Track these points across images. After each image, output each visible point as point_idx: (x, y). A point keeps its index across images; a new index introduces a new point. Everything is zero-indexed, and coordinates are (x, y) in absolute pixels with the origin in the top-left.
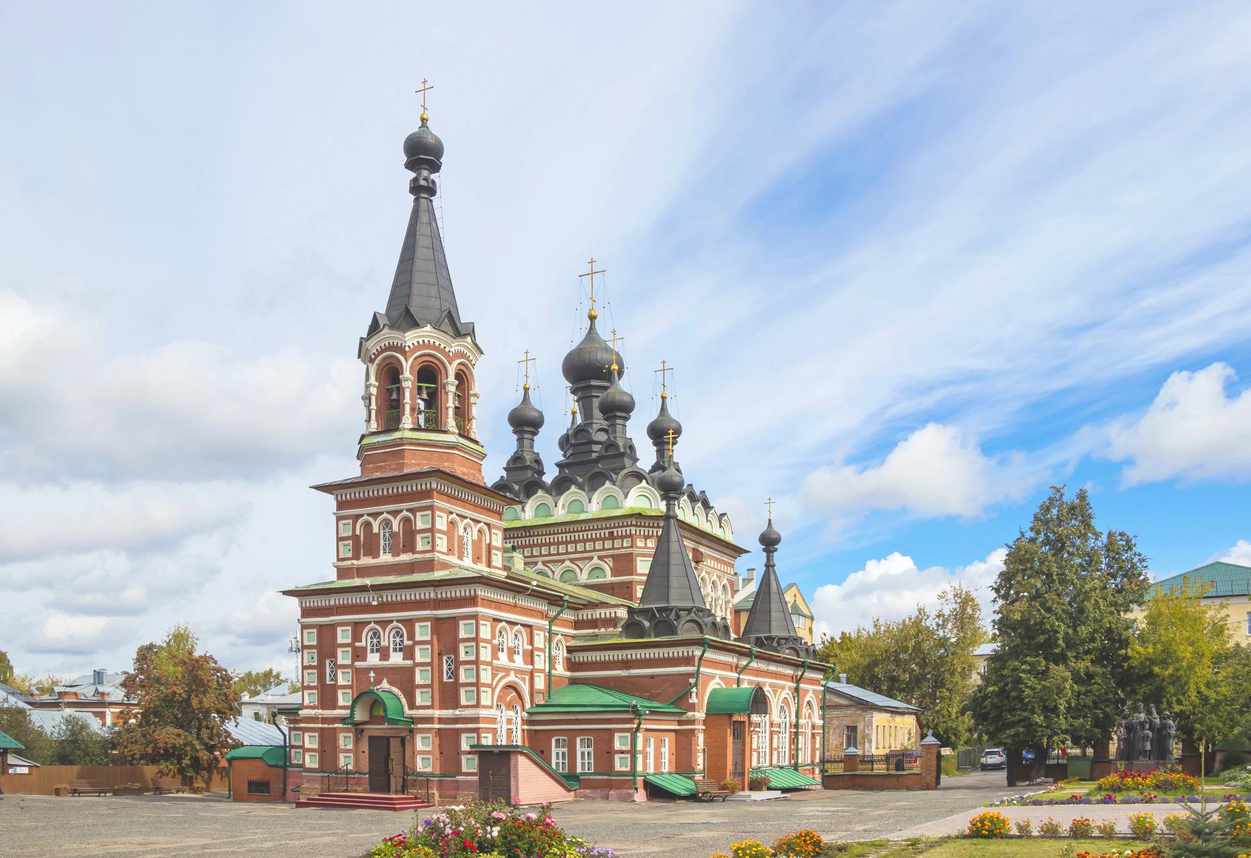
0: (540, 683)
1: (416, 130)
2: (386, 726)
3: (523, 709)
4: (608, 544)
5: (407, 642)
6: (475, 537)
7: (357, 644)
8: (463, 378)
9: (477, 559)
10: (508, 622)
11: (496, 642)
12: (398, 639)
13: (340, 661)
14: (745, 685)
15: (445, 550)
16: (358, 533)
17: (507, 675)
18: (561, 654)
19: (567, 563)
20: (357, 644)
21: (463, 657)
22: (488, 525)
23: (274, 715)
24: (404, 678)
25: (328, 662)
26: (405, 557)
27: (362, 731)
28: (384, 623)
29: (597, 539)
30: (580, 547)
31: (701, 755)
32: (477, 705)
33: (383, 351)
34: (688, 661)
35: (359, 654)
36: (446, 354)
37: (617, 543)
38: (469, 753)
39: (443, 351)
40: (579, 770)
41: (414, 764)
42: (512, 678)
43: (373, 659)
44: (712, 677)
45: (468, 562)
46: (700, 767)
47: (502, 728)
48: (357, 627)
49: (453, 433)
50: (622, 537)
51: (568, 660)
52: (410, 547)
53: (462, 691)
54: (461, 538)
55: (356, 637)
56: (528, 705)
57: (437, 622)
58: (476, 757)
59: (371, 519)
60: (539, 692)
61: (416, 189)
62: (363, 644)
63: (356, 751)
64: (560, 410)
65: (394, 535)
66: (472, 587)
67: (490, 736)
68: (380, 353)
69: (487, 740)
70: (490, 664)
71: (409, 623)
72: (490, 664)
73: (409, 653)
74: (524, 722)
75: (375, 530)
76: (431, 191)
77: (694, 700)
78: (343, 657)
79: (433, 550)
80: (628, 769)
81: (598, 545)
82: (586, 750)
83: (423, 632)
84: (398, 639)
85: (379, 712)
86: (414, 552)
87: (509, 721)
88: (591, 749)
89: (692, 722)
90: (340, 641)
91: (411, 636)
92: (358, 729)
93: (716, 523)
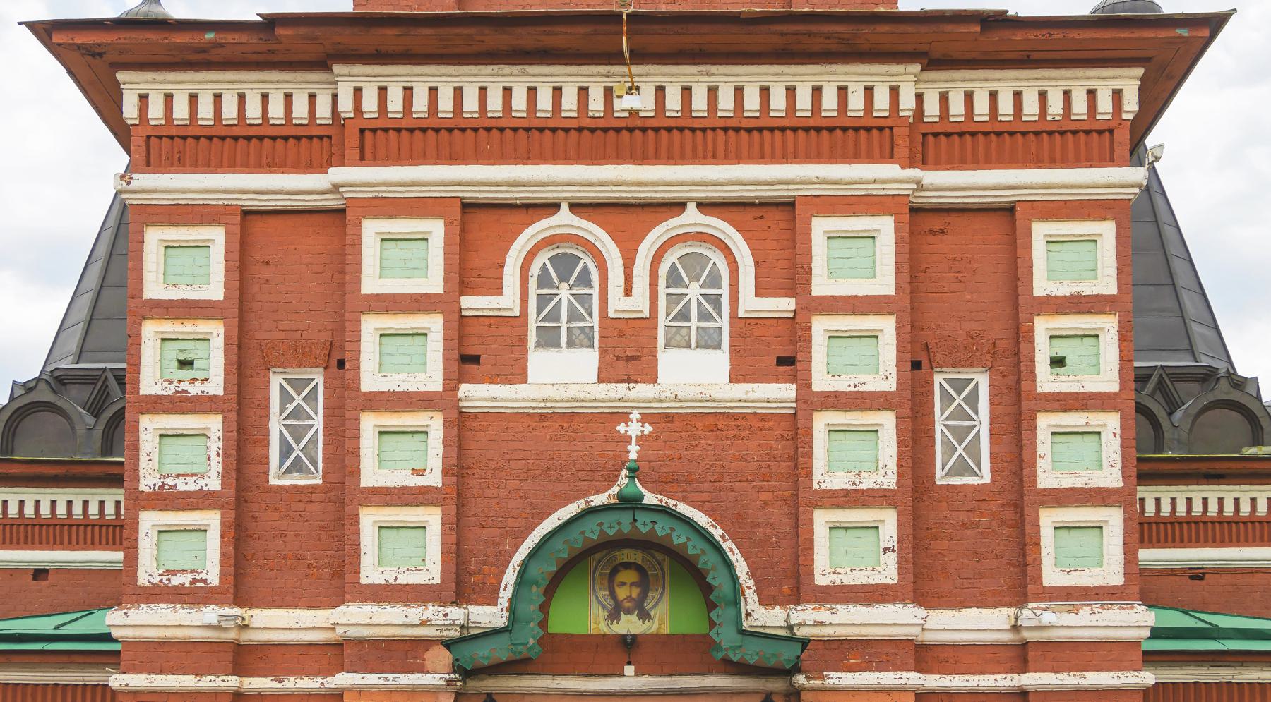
5: (752, 304)
7: (473, 303)
12: (694, 291)
20: (473, 303)
24: (765, 467)
43: (562, 375)
62: (506, 302)
73: (776, 350)
78: (405, 357)
91: (787, 269)
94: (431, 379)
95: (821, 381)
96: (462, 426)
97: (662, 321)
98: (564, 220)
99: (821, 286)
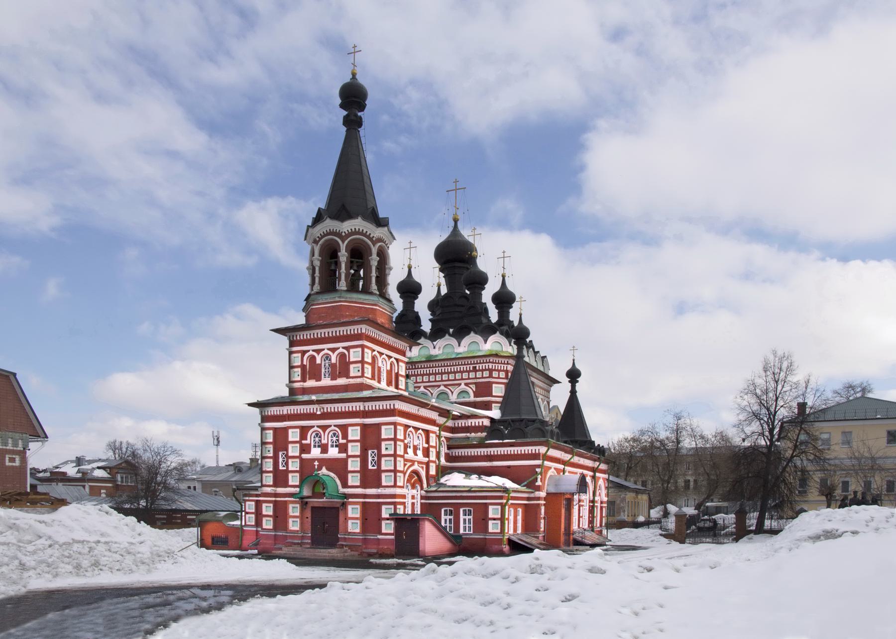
0: (433, 472)
1: (348, 80)
2: (325, 499)
3: (422, 488)
4: (472, 375)
5: (342, 441)
6: (389, 368)
7: (304, 442)
8: (383, 256)
9: (389, 383)
10: (414, 428)
11: (406, 441)
12: (334, 439)
13: (290, 454)
14: (567, 474)
15: (370, 376)
16: (305, 363)
17: (413, 465)
18: (444, 450)
19: (442, 388)
20: (304, 442)
21: (384, 452)
22: (397, 360)
23: (234, 490)
24: (339, 467)
25: (281, 453)
26: (342, 381)
27: (307, 503)
28: (324, 428)
29: (464, 372)
30: (451, 377)
31: (542, 521)
32: (395, 486)
33: (325, 235)
34: (535, 456)
36: (371, 239)
37: (479, 374)
38: (388, 519)
39: (368, 237)
40: (462, 531)
41: (346, 528)
42: (416, 467)
43: (316, 452)
44: (550, 468)
45: (383, 385)
46: (542, 529)
47: (409, 501)
48: (304, 431)
49: (375, 294)
50: (482, 371)
51: (447, 455)
53: (383, 475)
54: (379, 368)
55: (303, 436)
56: (425, 485)
57: (364, 427)
58: (392, 523)
59: (315, 354)
60: (432, 476)
61: (347, 121)
62: (308, 442)
63: (302, 517)
64: (432, 282)
65: (333, 366)
66: (392, 402)
67: (401, 507)
68: (323, 237)
69: (400, 510)
70: (402, 456)
71: (344, 428)
72: (402, 456)
73: (343, 448)
74: (422, 498)
75: (318, 361)
76: (359, 123)
77: (539, 483)
78: (294, 450)
79: (363, 376)
80: (499, 531)
81: (465, 375)
82: (467, 517)
83: (354, 433)
84: (334, 439)
85: (319, 489)
86: (348, 377)
87: (413, 497)
88: (471, 517)
89: (539, 499)
90: (290, 439)
91: (345, 436)
92: (304, 503)
93: (540, 363)
94: (297, 454)
95: (350, 453)
96: (302, 461)
97: (330, 443)
98: (316, 428)
99: (350, 438)
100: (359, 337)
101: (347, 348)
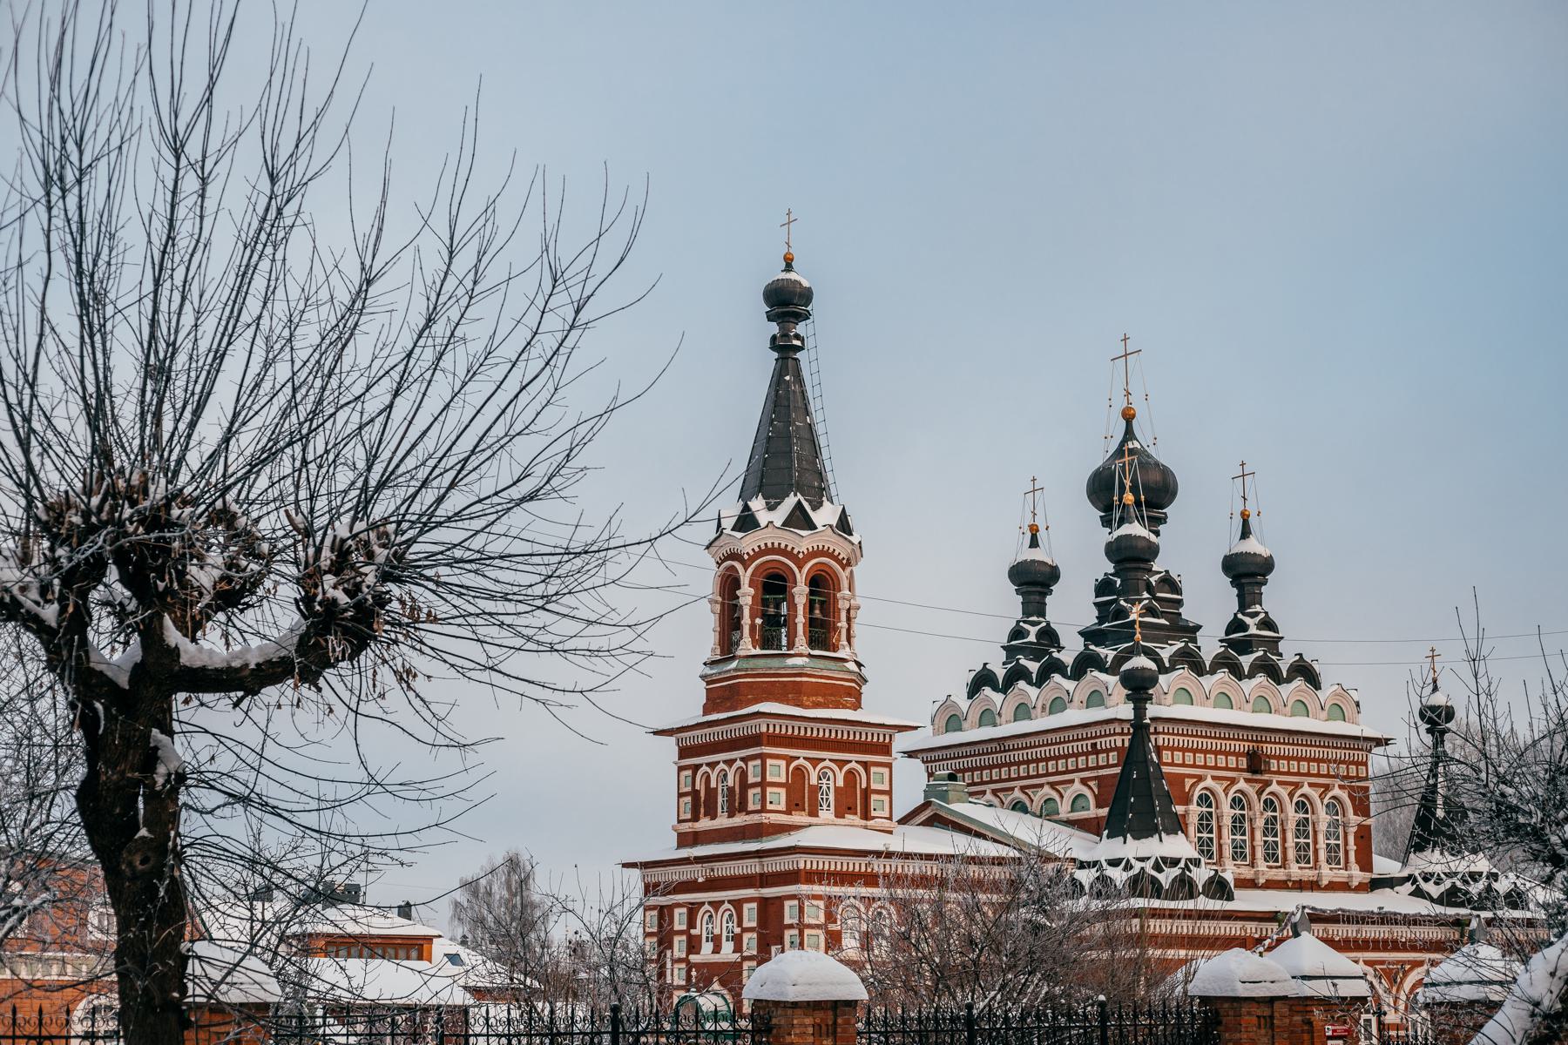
6: (840, 783)
22: (866, 765)
35: (693, 945)
50: (1107, 751)
52: (743, 808)
86: (749, 813)
100: (755, 740)
101: (745, 760)
